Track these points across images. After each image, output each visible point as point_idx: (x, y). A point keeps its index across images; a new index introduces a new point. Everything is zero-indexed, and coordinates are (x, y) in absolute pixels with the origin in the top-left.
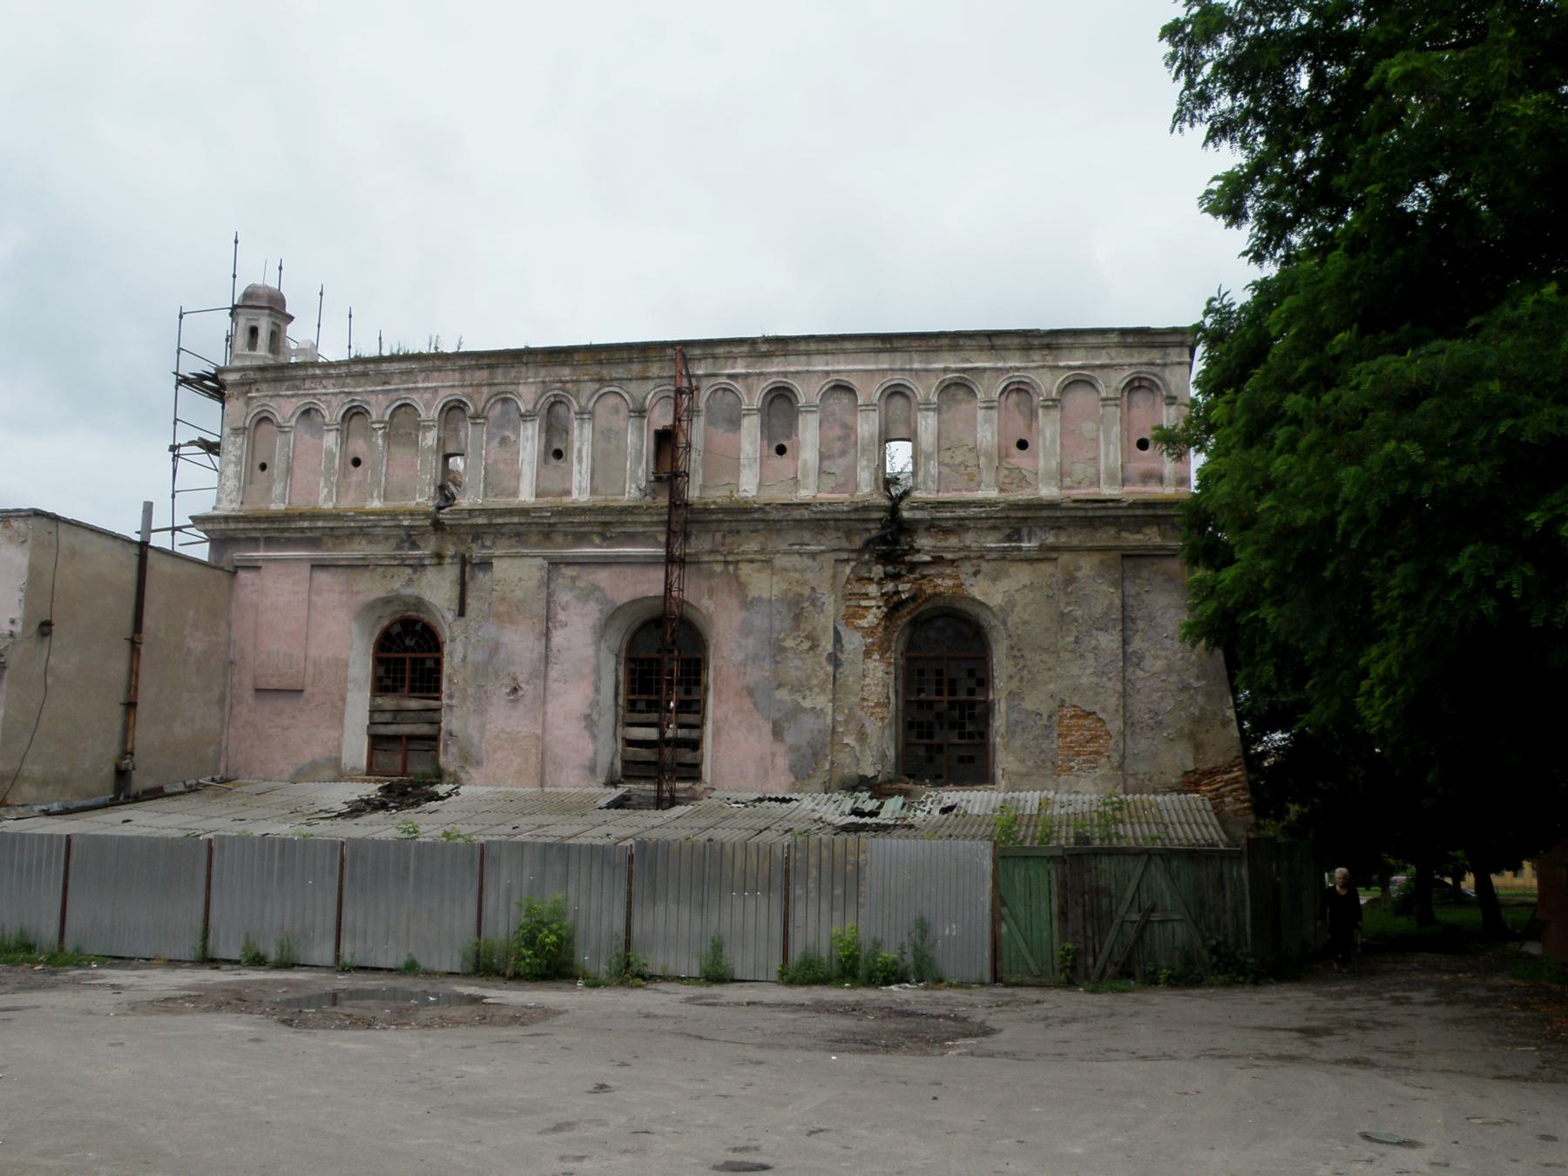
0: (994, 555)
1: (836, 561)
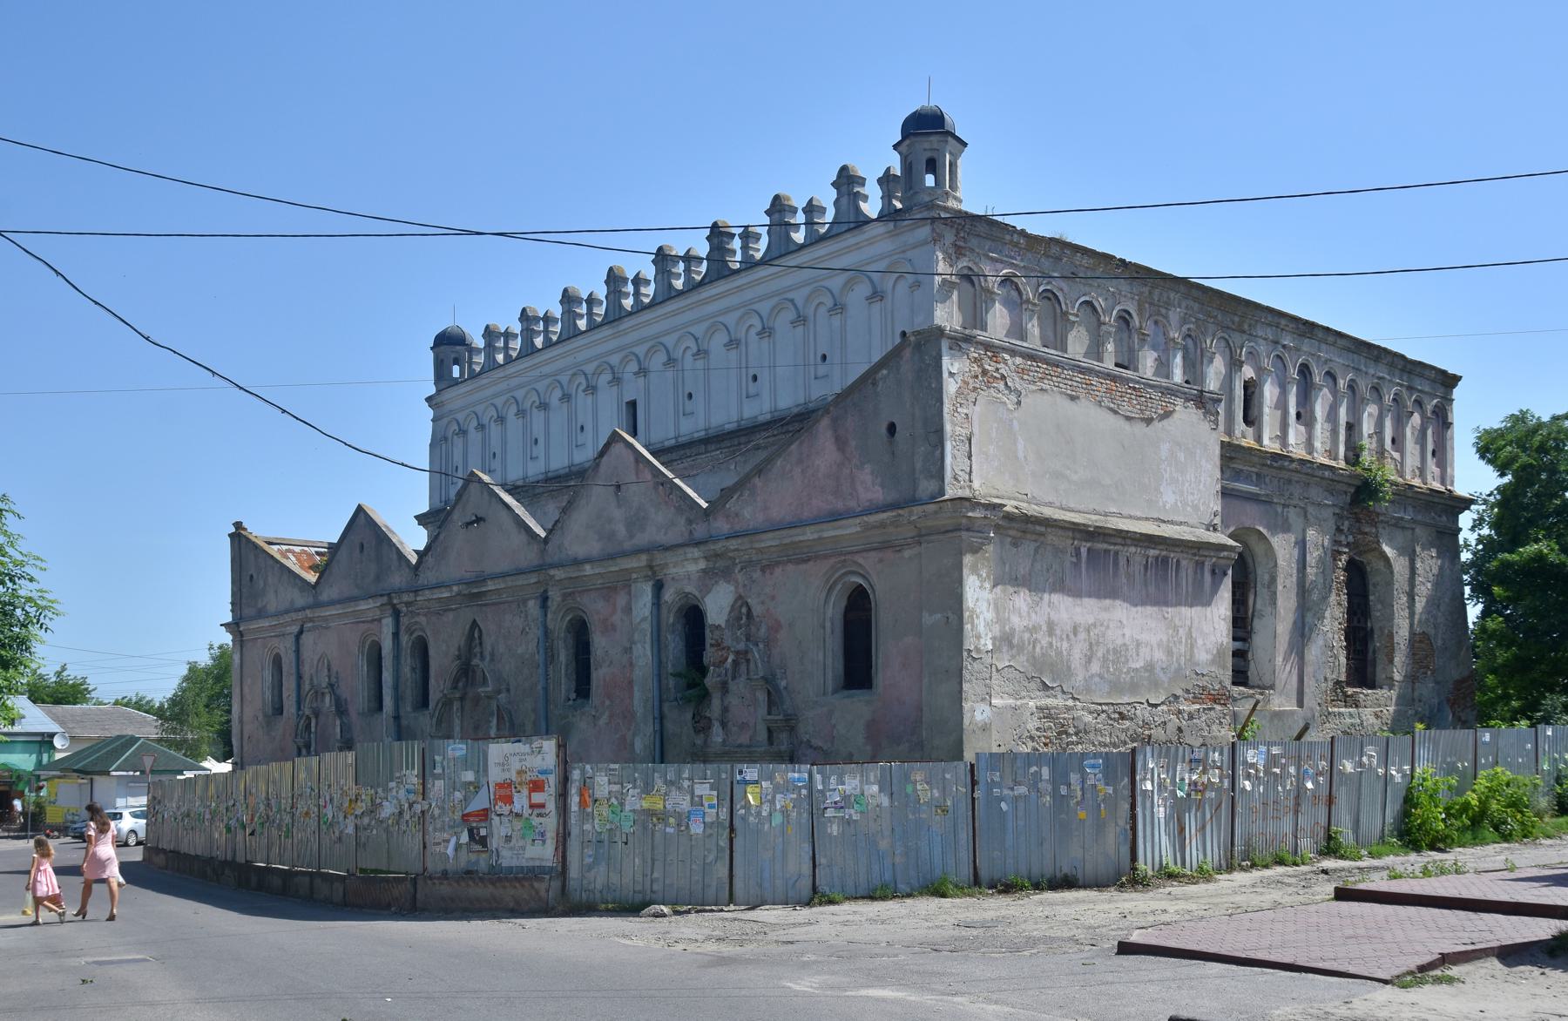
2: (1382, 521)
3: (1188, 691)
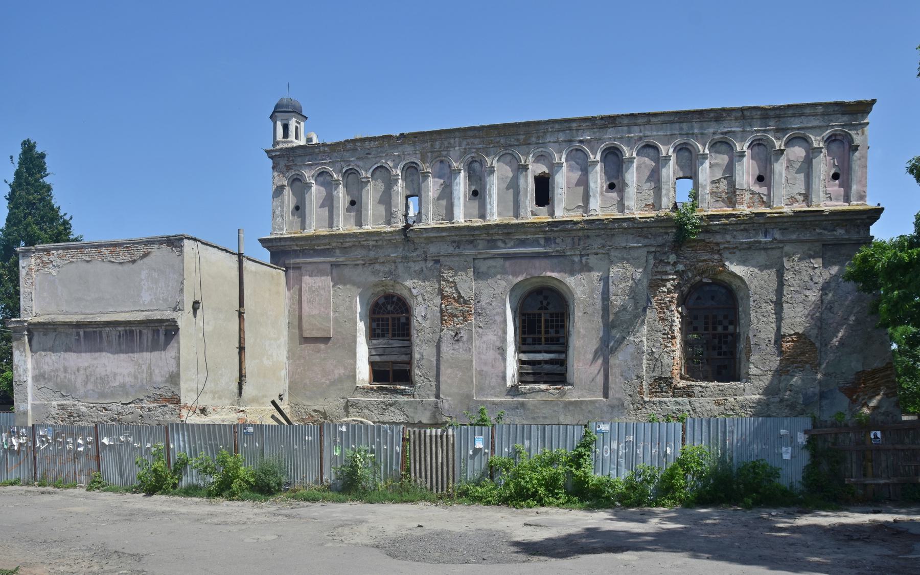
0: (745, 246)
1: (648, 252)
2: (725, 248)
3: (149, 397)
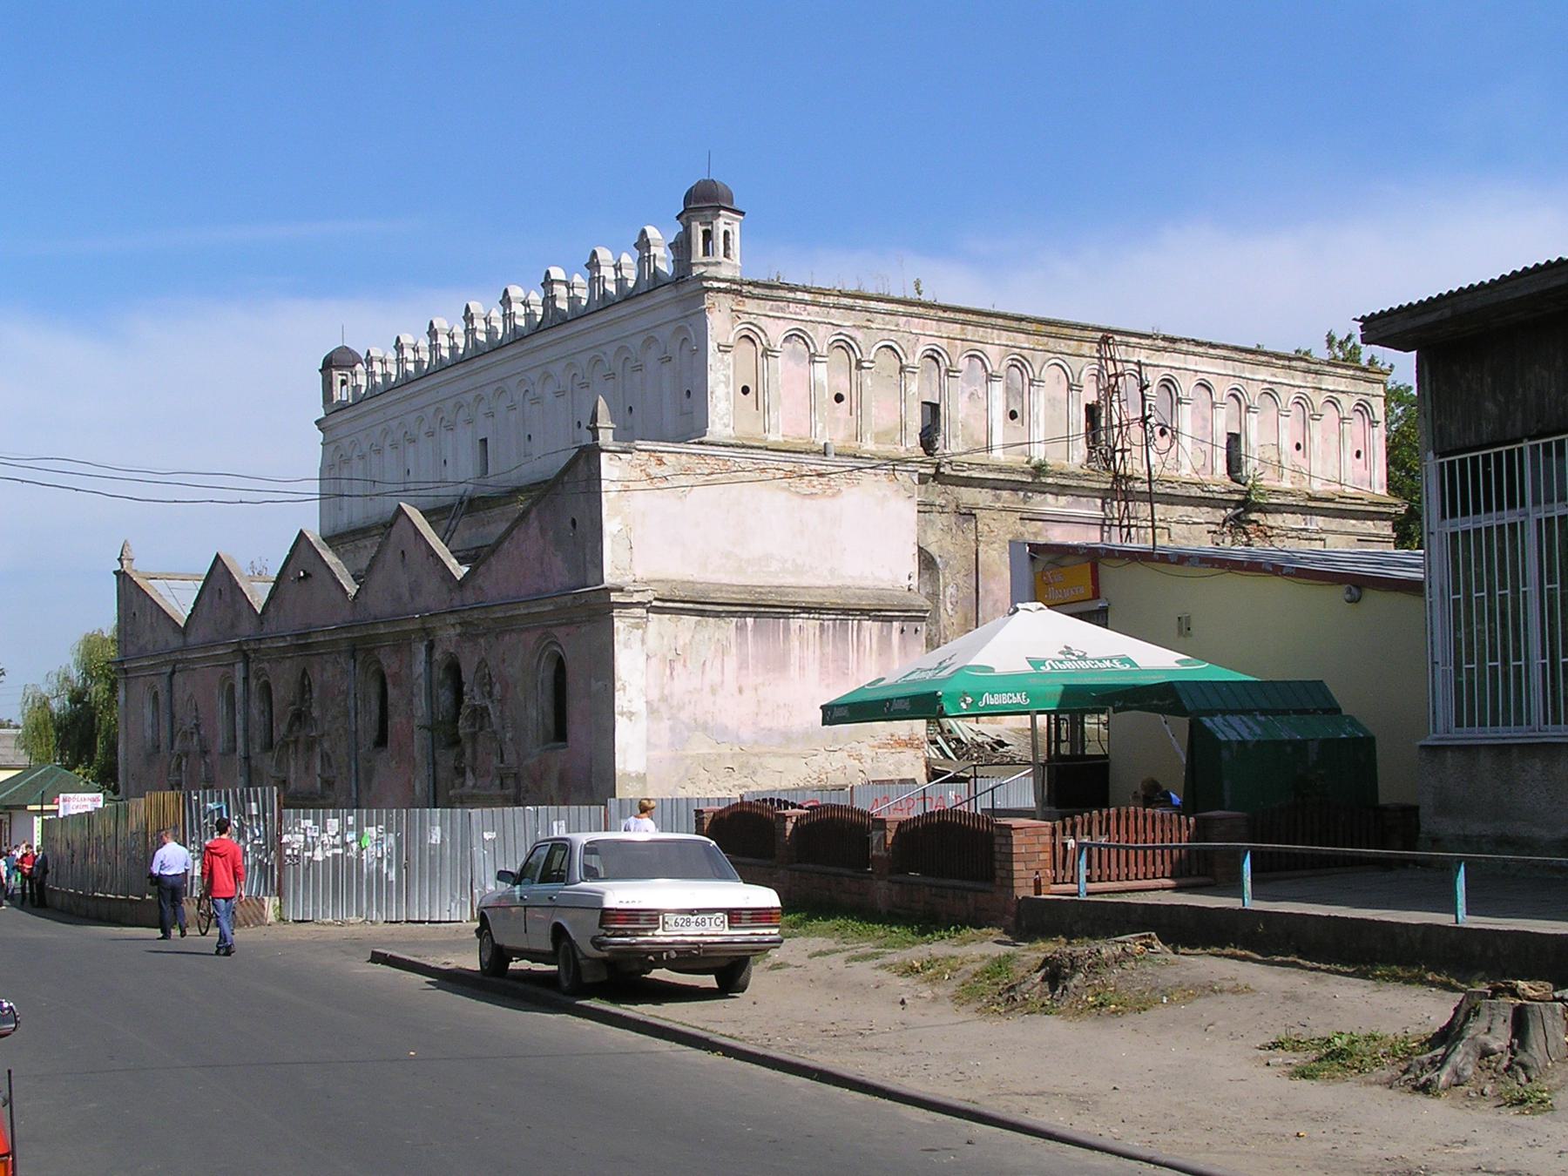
2: (1278, 535)
